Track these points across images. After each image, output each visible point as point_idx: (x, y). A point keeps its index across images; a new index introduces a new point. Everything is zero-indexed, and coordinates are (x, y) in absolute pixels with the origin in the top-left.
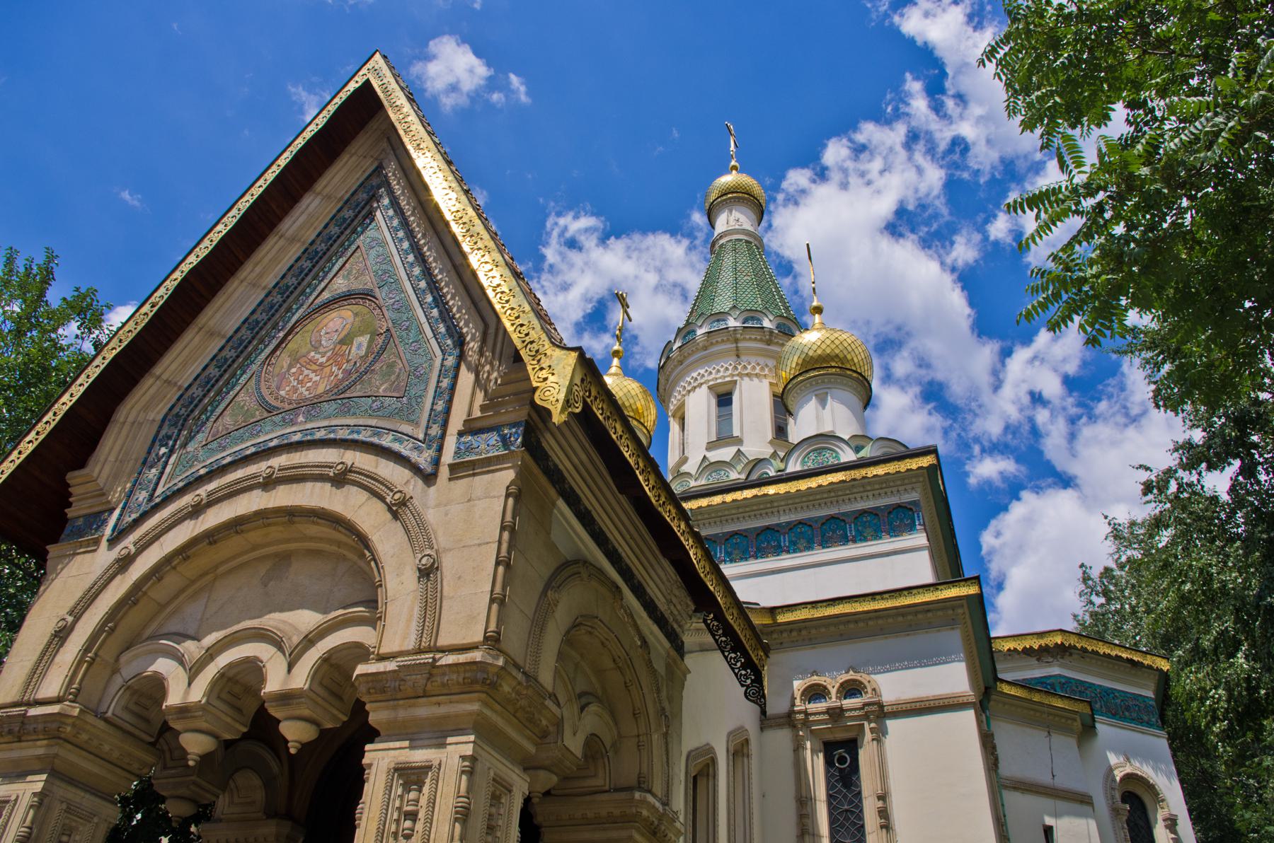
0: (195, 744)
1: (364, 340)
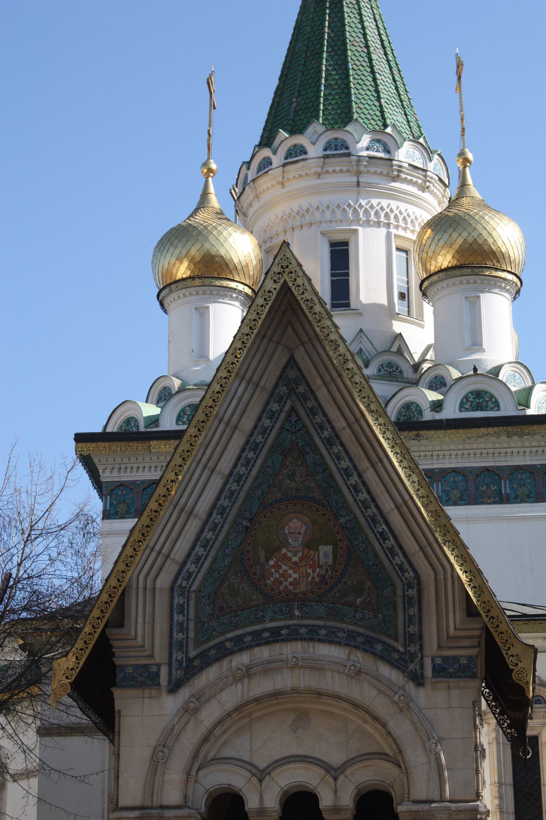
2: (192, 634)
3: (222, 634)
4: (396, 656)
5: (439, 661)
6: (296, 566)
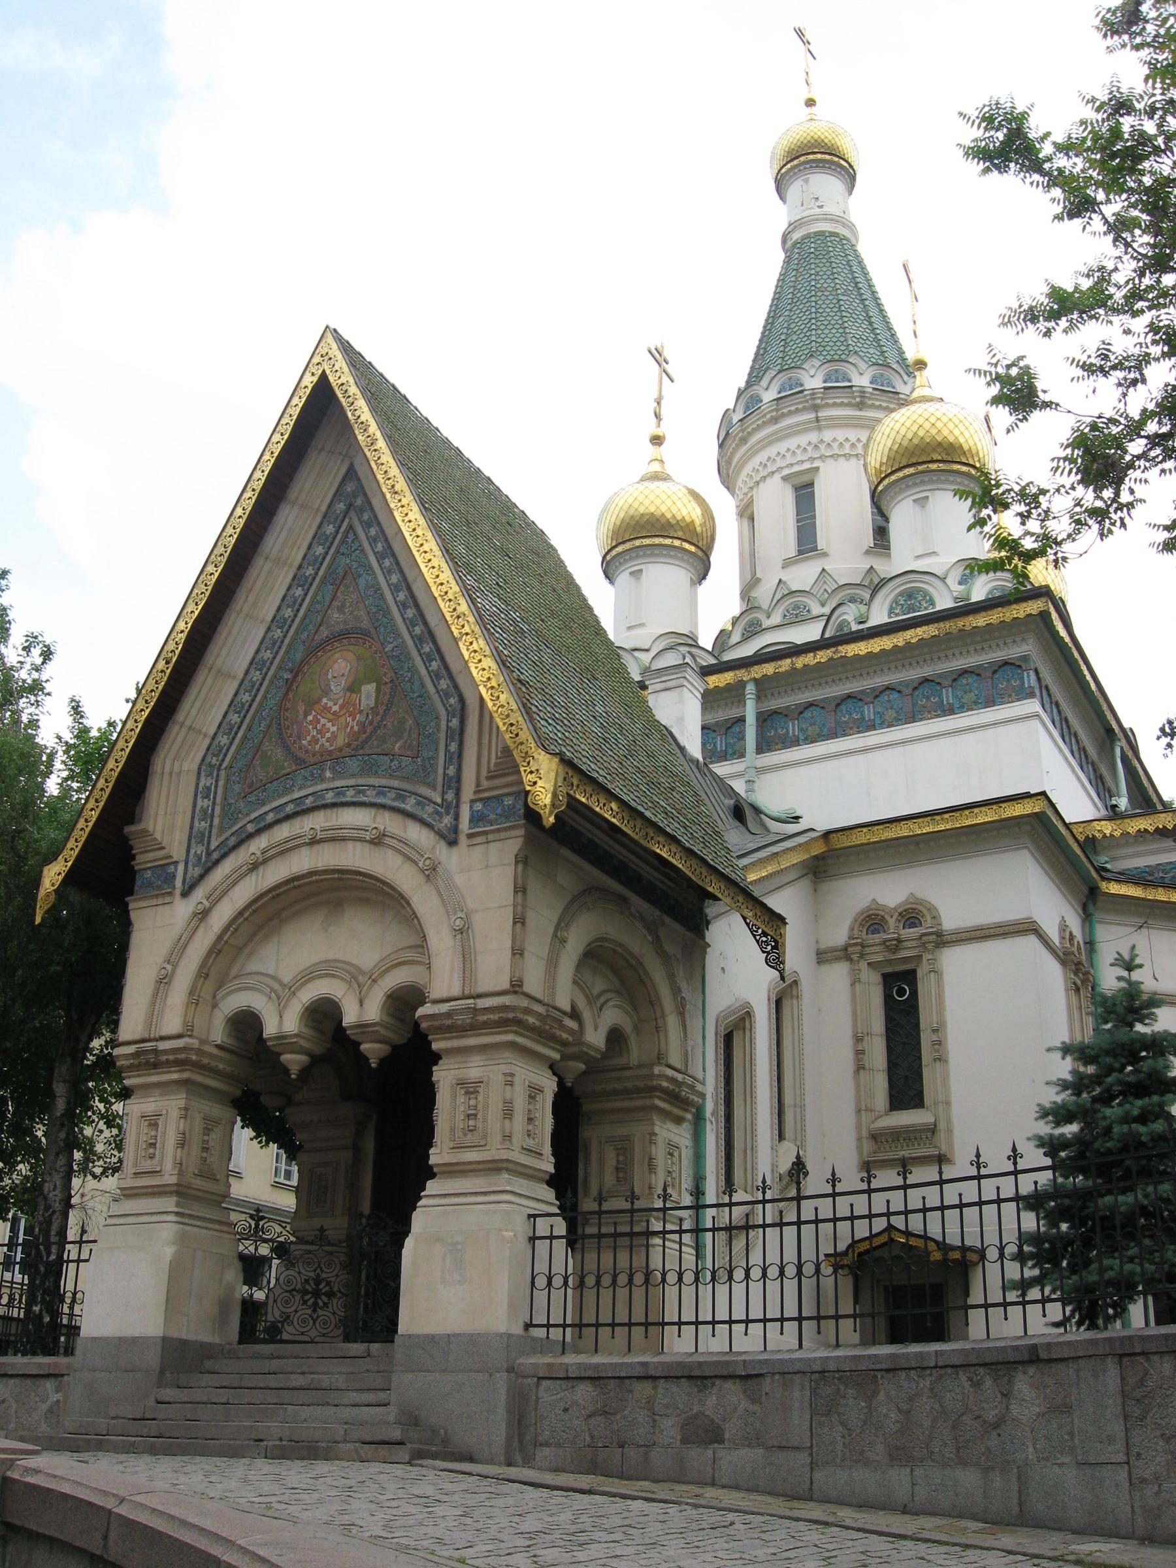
0: (293, 1061)
1: (369, 689)
2: (216, 821)
4: (430, 809)
5: (479, 806)
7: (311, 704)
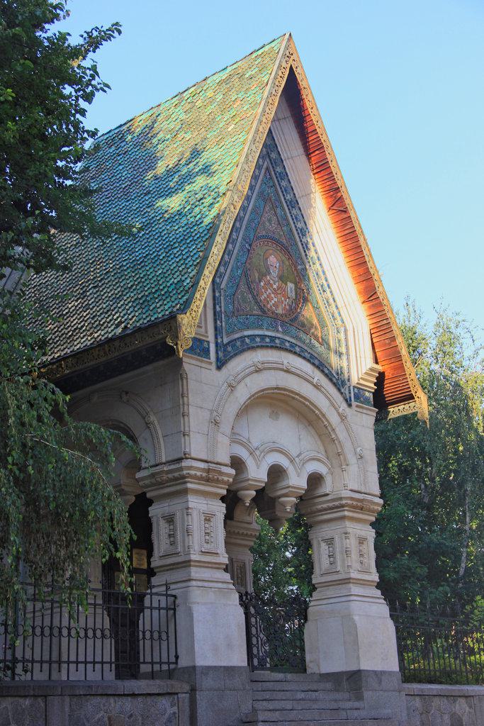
3: (241, 330)
6: (275, 291)
7: (262, 276)
